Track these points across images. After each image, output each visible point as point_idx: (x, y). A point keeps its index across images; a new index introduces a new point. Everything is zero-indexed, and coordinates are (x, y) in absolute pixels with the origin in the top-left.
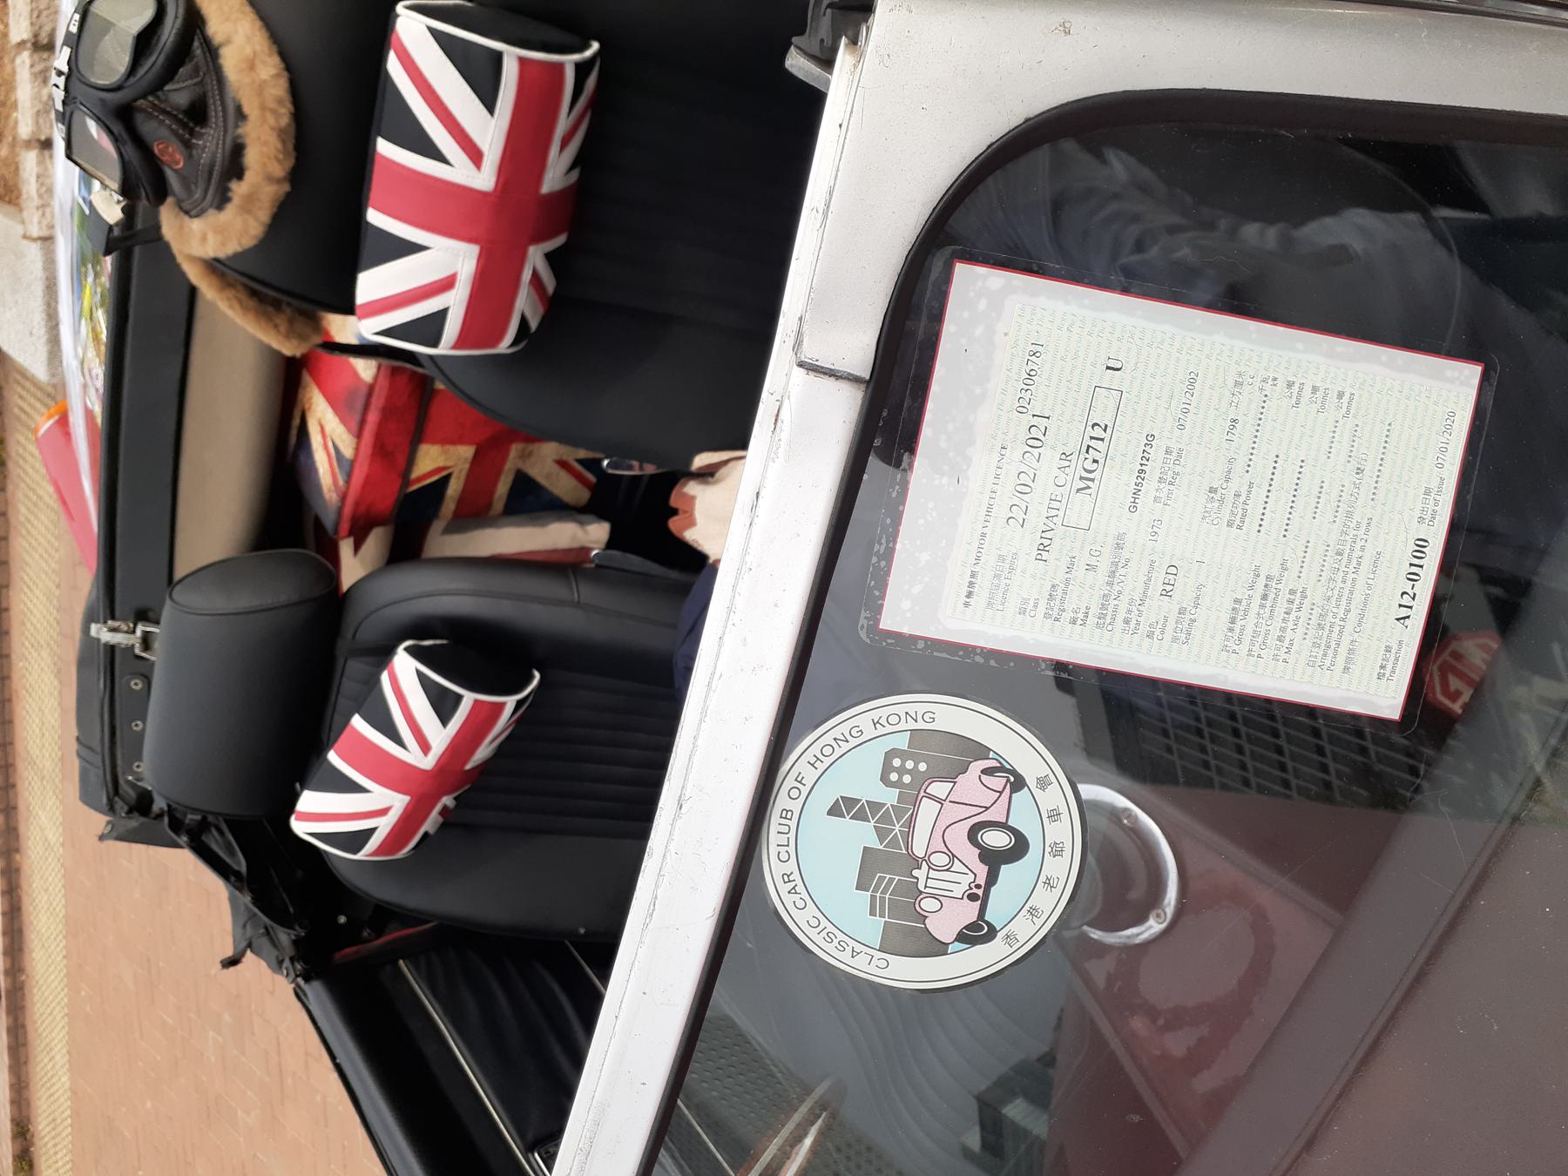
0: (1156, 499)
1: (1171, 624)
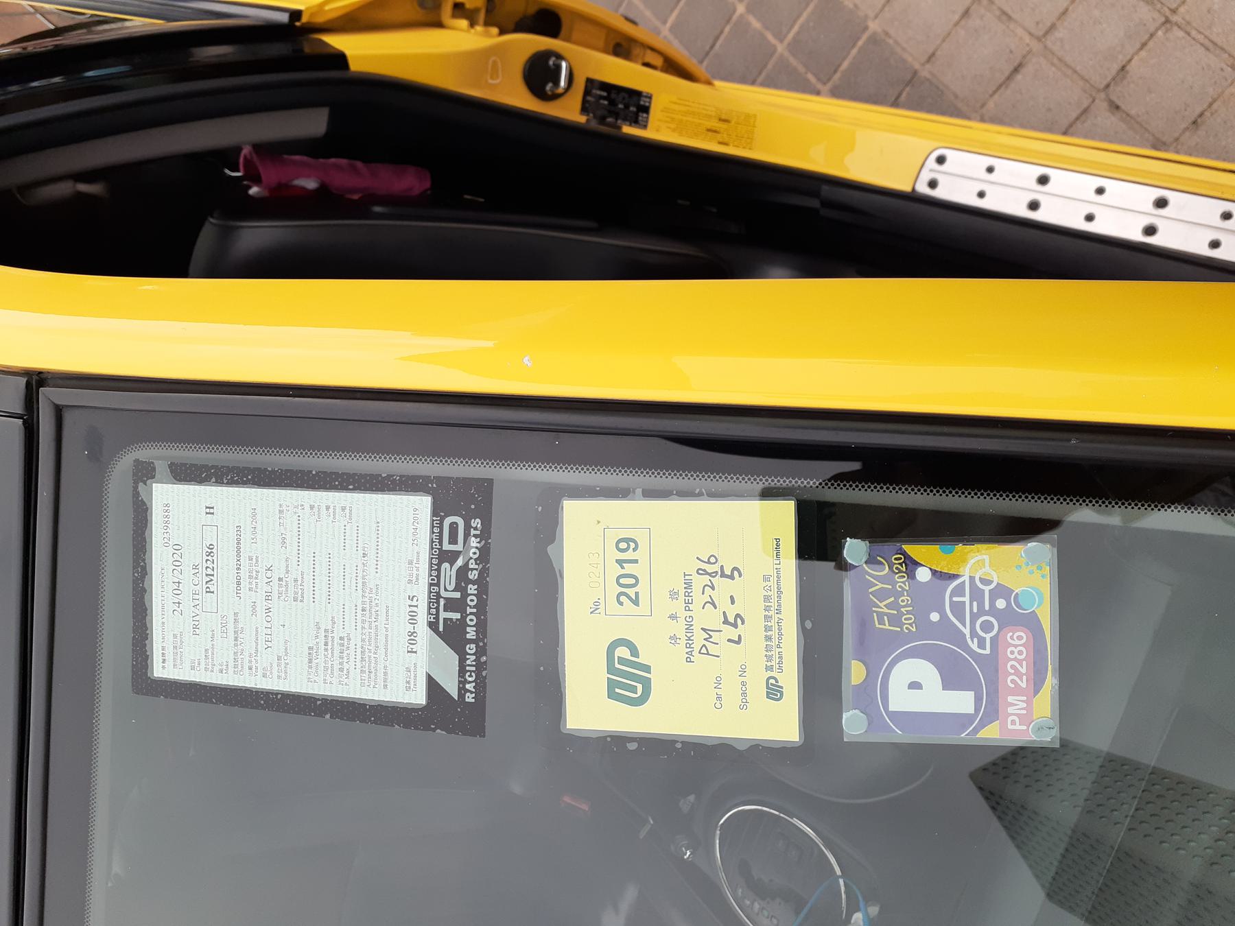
0: (250, 589)
1: (275, 665)
